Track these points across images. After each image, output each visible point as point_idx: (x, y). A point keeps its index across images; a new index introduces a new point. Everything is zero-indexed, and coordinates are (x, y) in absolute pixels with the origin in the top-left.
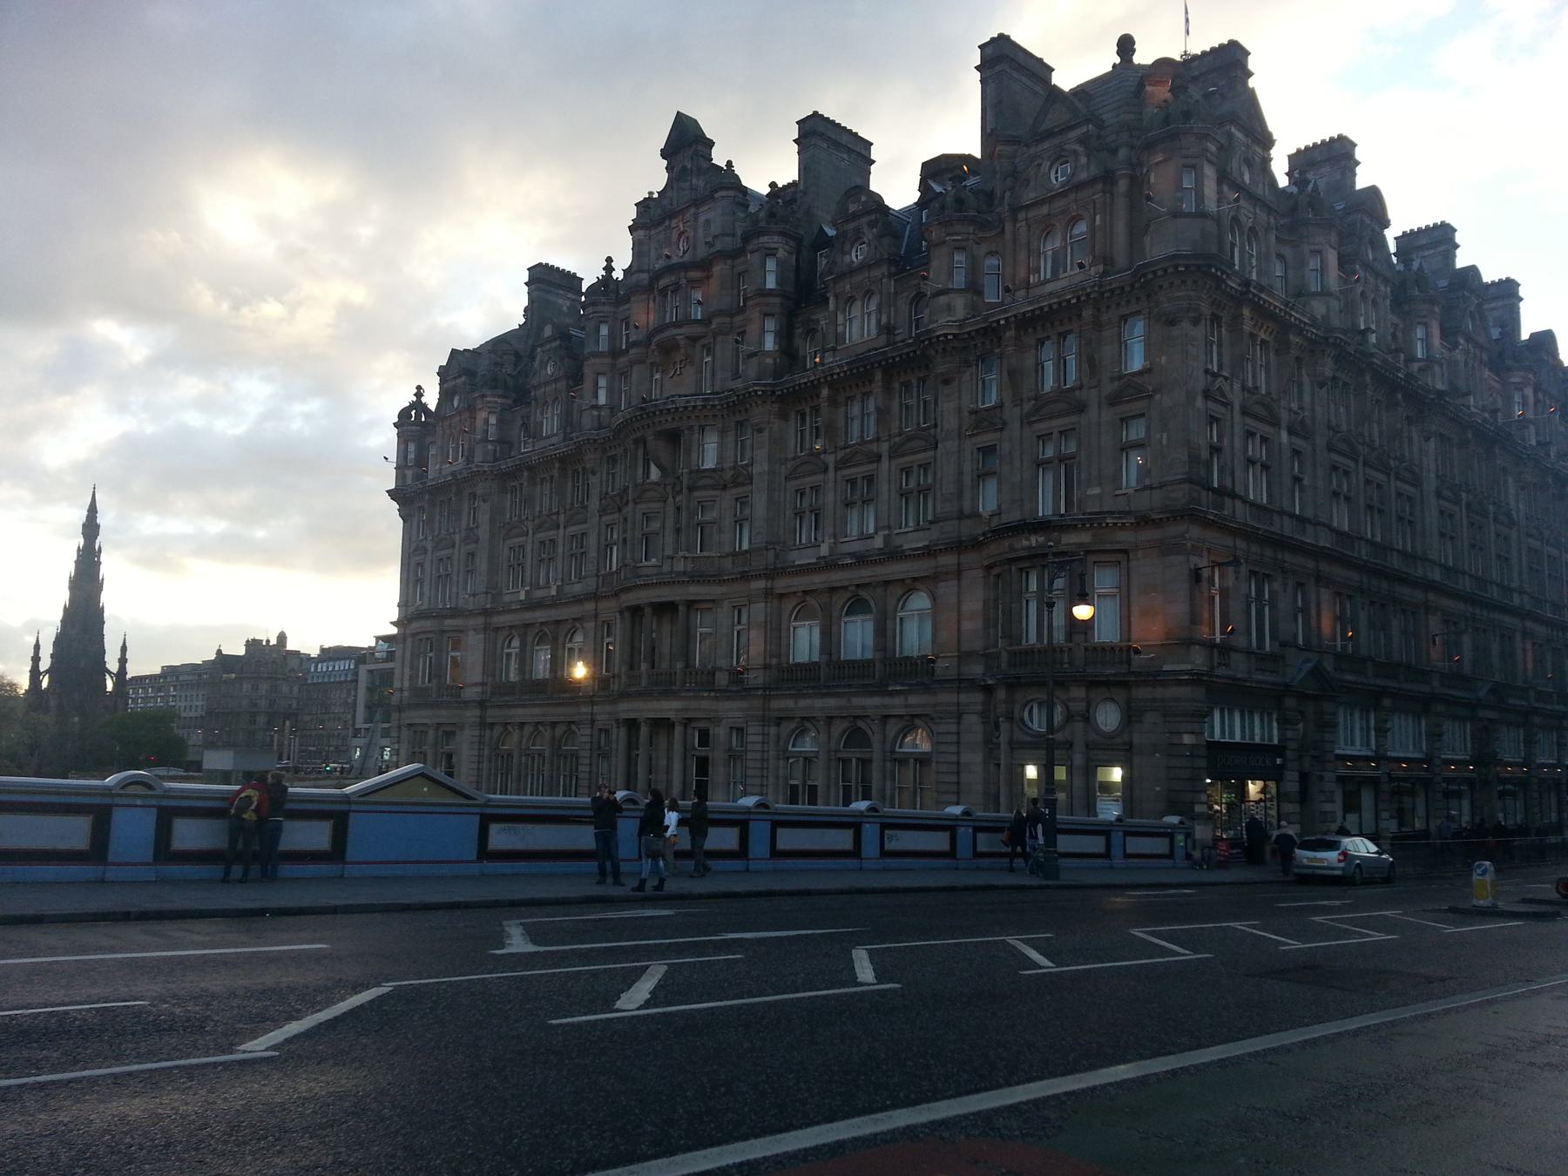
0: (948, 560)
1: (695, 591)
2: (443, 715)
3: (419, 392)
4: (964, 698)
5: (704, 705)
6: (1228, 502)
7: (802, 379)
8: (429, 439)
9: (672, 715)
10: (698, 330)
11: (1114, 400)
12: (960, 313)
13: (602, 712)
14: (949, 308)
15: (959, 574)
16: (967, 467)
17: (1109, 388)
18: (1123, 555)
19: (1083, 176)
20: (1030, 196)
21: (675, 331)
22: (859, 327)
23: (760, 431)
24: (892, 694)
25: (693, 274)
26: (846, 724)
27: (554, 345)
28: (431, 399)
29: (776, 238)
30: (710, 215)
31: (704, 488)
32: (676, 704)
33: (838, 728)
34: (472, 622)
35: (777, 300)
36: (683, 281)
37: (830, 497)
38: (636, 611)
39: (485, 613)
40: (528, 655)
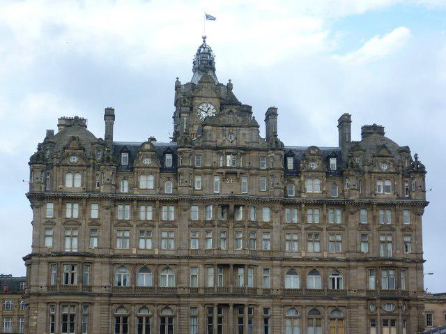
1: (251, 262)
4: (359, 302)
9: (245, 303)
11: (403, 230)
12: (357, 196)
17: (401, 227)
19: (392, 171)
20: (377, 170)
21: (237, 170)
22: (313, 187)
23: (277, 212)
25: (241, 151)
26: (312, 308)
30: (245, 132)
31: (254, 227)
32: (247, 299)
33: (308, 309)
39: (112, 257)
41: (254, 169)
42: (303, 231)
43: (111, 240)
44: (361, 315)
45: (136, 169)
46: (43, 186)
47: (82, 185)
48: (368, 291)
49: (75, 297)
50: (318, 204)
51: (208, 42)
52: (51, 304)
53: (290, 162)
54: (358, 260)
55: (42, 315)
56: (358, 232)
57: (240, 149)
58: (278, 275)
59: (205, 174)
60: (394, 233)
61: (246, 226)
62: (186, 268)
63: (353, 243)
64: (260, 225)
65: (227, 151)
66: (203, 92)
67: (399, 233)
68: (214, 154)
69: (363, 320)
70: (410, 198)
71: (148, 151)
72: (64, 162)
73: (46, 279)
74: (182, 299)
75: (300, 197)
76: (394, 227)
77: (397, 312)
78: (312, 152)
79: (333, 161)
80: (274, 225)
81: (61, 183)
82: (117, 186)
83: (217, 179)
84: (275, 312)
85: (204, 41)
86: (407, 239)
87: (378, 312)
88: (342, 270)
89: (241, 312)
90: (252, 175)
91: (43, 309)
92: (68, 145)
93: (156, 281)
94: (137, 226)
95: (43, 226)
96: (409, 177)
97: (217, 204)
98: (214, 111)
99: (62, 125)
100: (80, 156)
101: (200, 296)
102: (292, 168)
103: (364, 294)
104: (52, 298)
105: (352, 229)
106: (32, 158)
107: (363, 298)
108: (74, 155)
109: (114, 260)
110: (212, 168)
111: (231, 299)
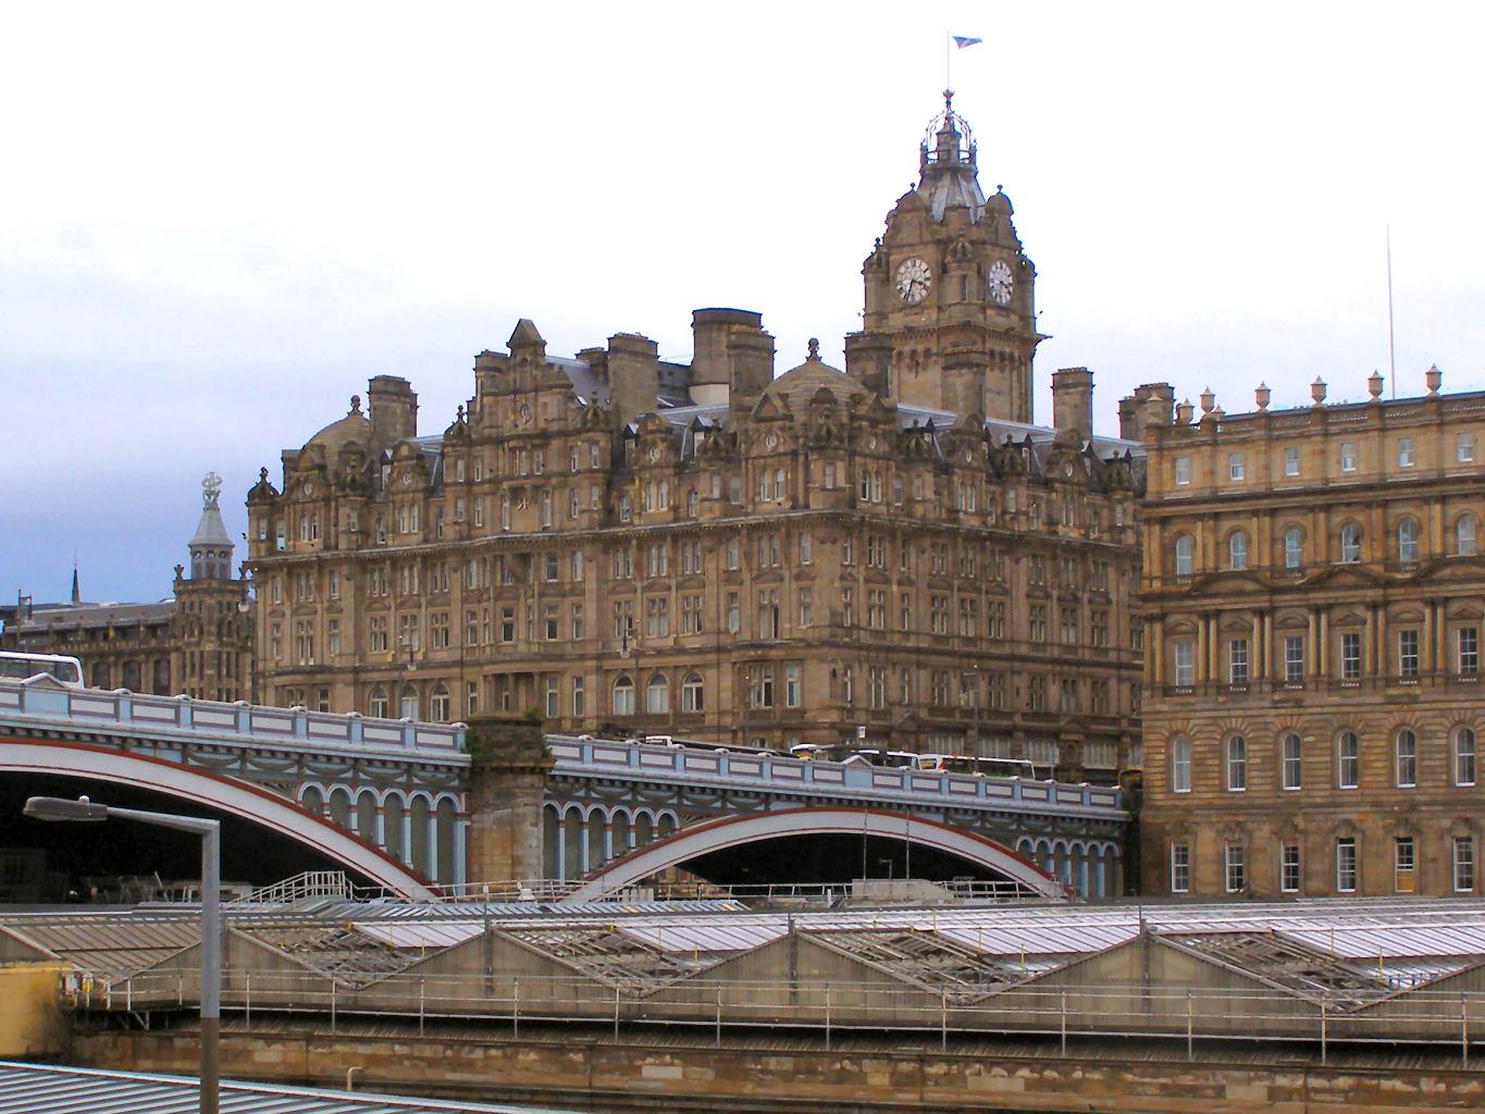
0: (712, 657)
6: (855, 632)
7: (619, 530)
8: (276, 516)
10: (541, 482)
11: (798, 577)
14: (711, 510)
15: (718, 665)
16: (722, 603)
17: (795, 571)
18: (800, 661)
19: (781, 450)
20: (754, 452)
22: (655, 503)
25: (536, 441)
27: (410, 462)
28: (277, 481)
29: (598, 434)
34: (341, 676)
35: (601, 475)
36: (529, 447)
38: (500, 677)
39: (356, 670)
40: (396, 705)
46: (262, 546)
50: (657, 536)
54: (719, 649)
65: (512, 444)
66: (907, 235)
78: (650, 427)
82: (365, 534)
85: (948, 103)
90: (554, 488)
97: (489, 557)
98: (928, 274)
108: (307, 480)
109: (364, 677)
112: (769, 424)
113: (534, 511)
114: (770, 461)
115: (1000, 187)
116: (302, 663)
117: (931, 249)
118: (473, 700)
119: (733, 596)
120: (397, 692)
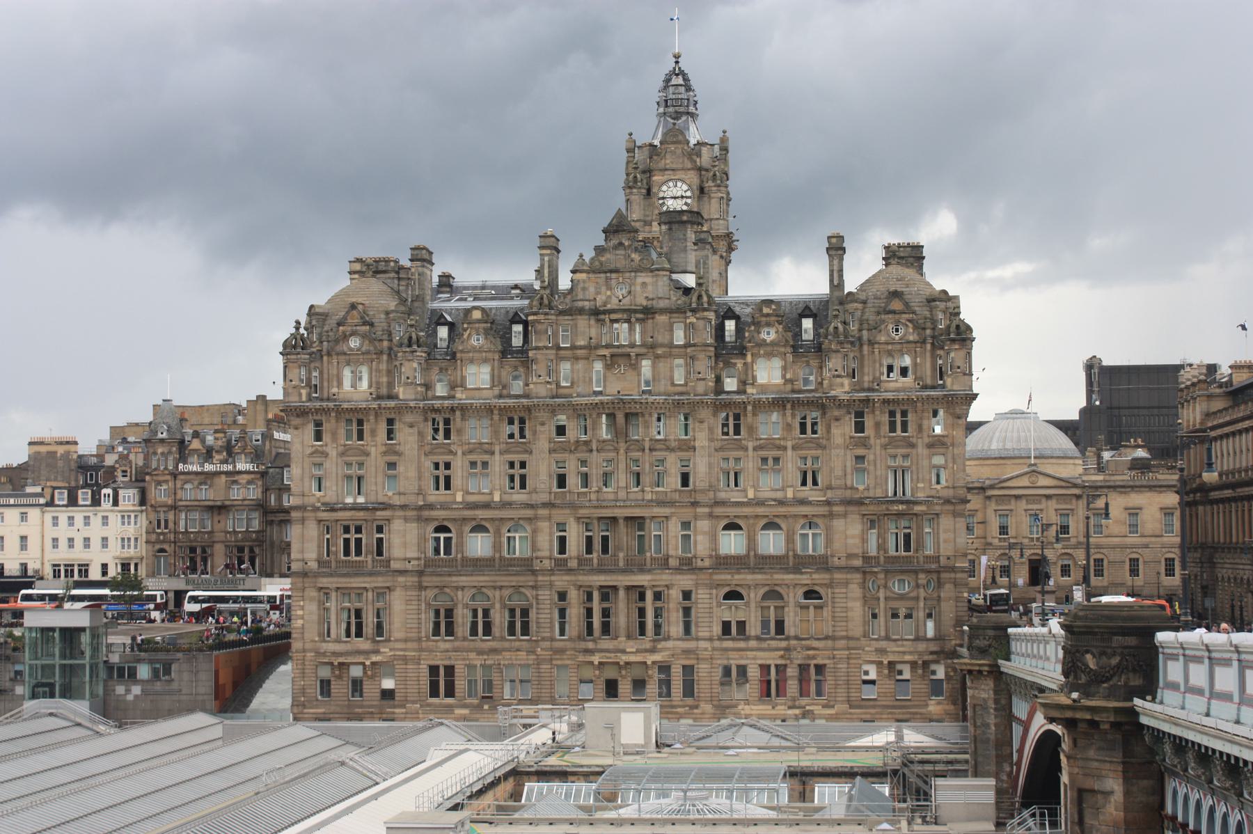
2: (380, 582)
3: (297, 329)
4: (849, 576)
5: (664, 578)
8: (312, 365)
9: (645, 584)
11: (930, 446)
12: (847, 388)
13: (561, 581)
14: (842, 385)
16: (849, 464)
17: (926, 440)
19: (911, 338)
20: (883, 339)
22: (769, 373)
24: (802, 573)
26: (767, 589)
31: (661, 450)
32: (648, 577)
33: (762, 591)
37: (751, 465)
39: (421, 508)
41: (662, 345)
42: (750, 452)
43: (420, 479)
44: (854, 599)
45: (458, 355)
46: (304, 392)
47: (370, 386)
48: (867, 559)
49: (361, 579)
50: (779, 404)
51: (682, 65)
52: (326, 592)
53: (730, 325)
54: (848, 502)
55: (312, 607)
56: (848, 452)
57: (635, 311)
58: (704, 533)
59: (577, 359)
60: (914, 451)
61: (647, 447)
62: (547, 524)
63: (838, 472)
64: (673, 444)
65: (614, 316)
66: (668, 161)
67: (922, 450)
68: (593, 322)
69: (857, 610)
70: (943, 386)
71: (479, 321)
72: (338, 348)
73: (315, 549)
74: (540, 578)
75: (744, 392)
76: (914, 440)
77: (913, 594)
78: (766, 310)
79: (807, 324)
80: (697, 444)
81: (335, 383)
82: (428, 386)
83: (598, 366)
84: (702, 597)
85: (677, 62)
86: (938, 460)
87: (881, 595)
88: (819, 521)
89: (642, 597)
91: (312, 599)
92: (345, 318)
93: (497, 546)
94: (464, 454)
95: (307, 459)
96: (942, 348)
99: (355, 272)
100: (364, 336)
101: (570, 571)
102: (733, 339)
103: (858, 563)
104: (324, 582)
105: (838, 447)
106: (286, 344)
107: (856, 569)
108: (353, 334)
109: (426, 513)
110: (589, 347)
111: (621, 578)
112: (897, 316)
113: (630, 374)
114: (898, 347)
115: (724, 132)
116: (349, 500)
117: (693, 177)
118: (562, 541)
119: (860, 459)
120: (468, 528)
